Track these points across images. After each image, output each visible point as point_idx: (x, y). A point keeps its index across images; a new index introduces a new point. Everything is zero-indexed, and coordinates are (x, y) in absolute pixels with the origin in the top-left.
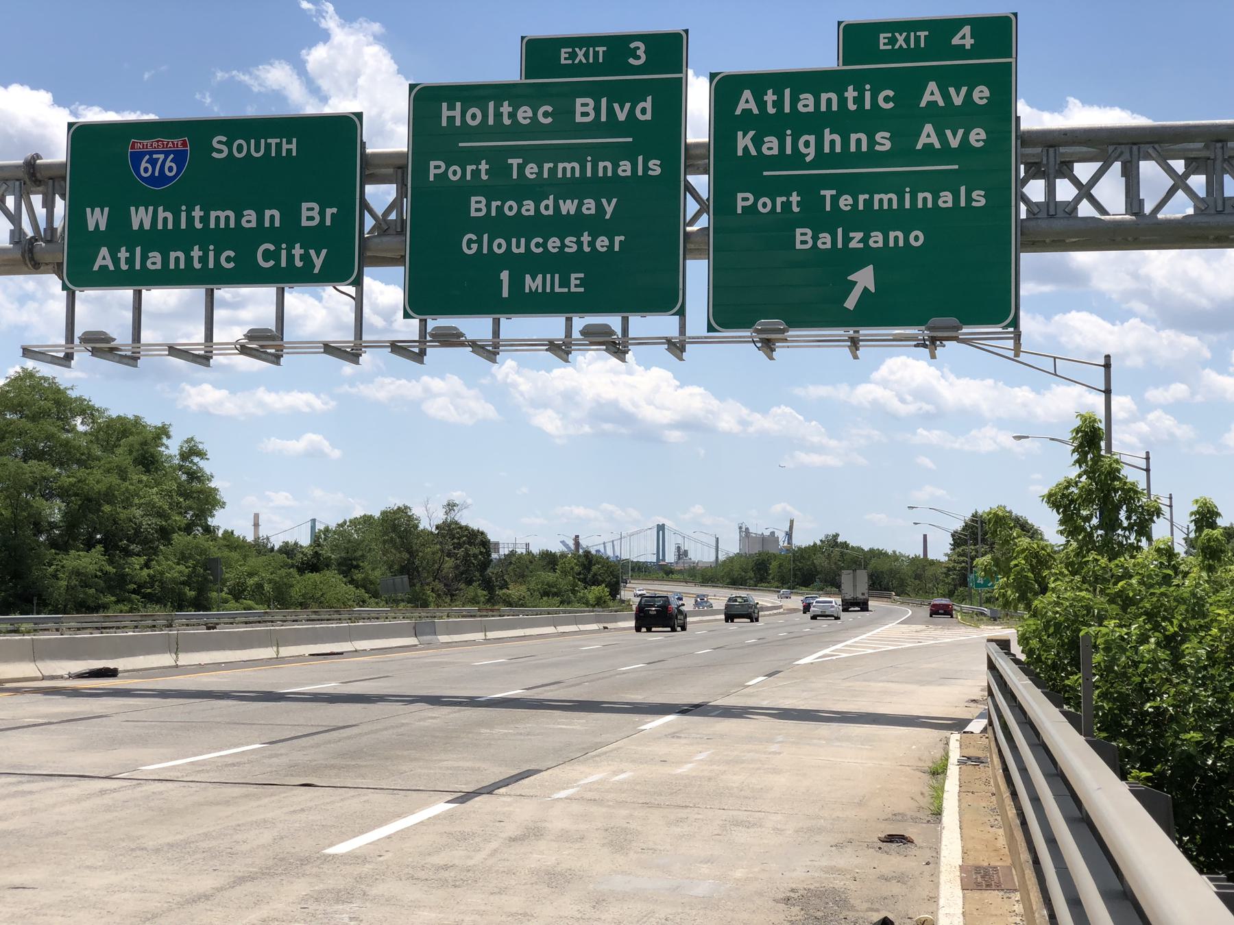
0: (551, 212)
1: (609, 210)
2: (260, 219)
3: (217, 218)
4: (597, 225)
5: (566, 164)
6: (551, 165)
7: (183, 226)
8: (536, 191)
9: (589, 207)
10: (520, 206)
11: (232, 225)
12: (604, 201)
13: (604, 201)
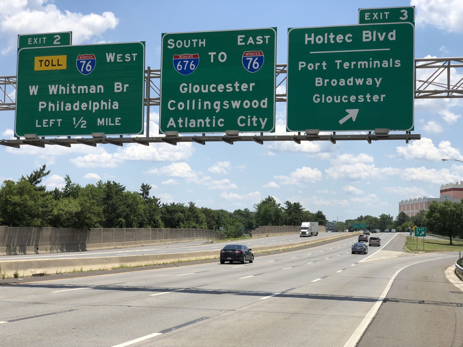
0: (352, 84)
1: (378, 83)
4: (373, 90)
5: (362, 62)
6: (355, 63)
8: (346, 74)
9: (369, 82)
10: (338, 81)
12: (376, 79)
13: (376, 79)
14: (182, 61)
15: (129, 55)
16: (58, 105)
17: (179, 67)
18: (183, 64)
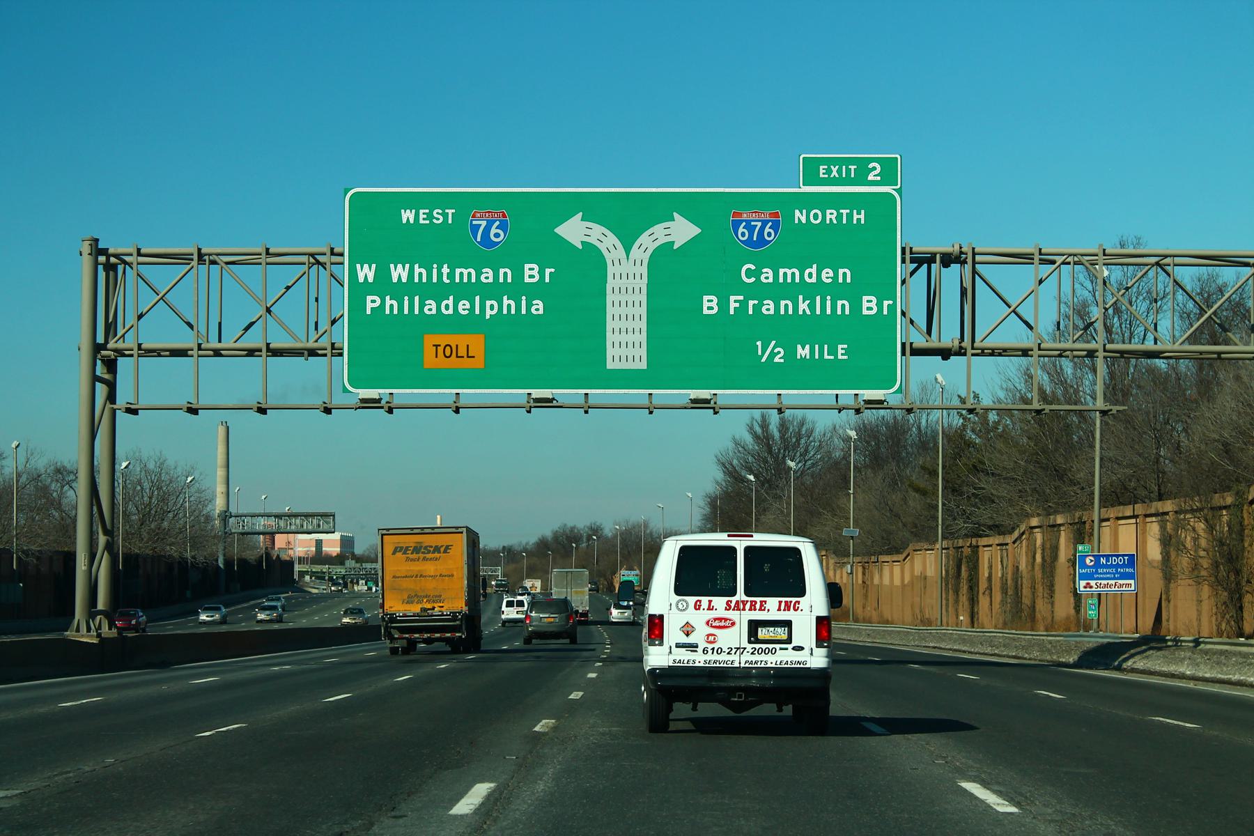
2: (496, 276)
3: (461, 274)
7: (435, 280)
11: (473, 280)
14: (748, 222)
15: (440, 211)
16: (406, 303)
17: (743, 234)
18: (751, 229)
